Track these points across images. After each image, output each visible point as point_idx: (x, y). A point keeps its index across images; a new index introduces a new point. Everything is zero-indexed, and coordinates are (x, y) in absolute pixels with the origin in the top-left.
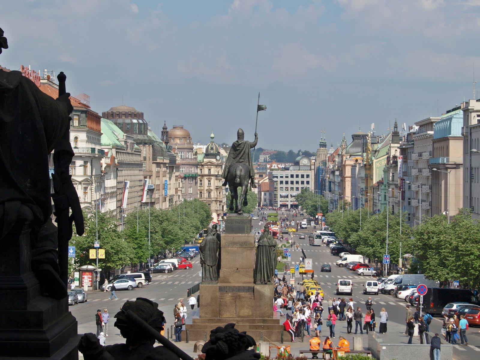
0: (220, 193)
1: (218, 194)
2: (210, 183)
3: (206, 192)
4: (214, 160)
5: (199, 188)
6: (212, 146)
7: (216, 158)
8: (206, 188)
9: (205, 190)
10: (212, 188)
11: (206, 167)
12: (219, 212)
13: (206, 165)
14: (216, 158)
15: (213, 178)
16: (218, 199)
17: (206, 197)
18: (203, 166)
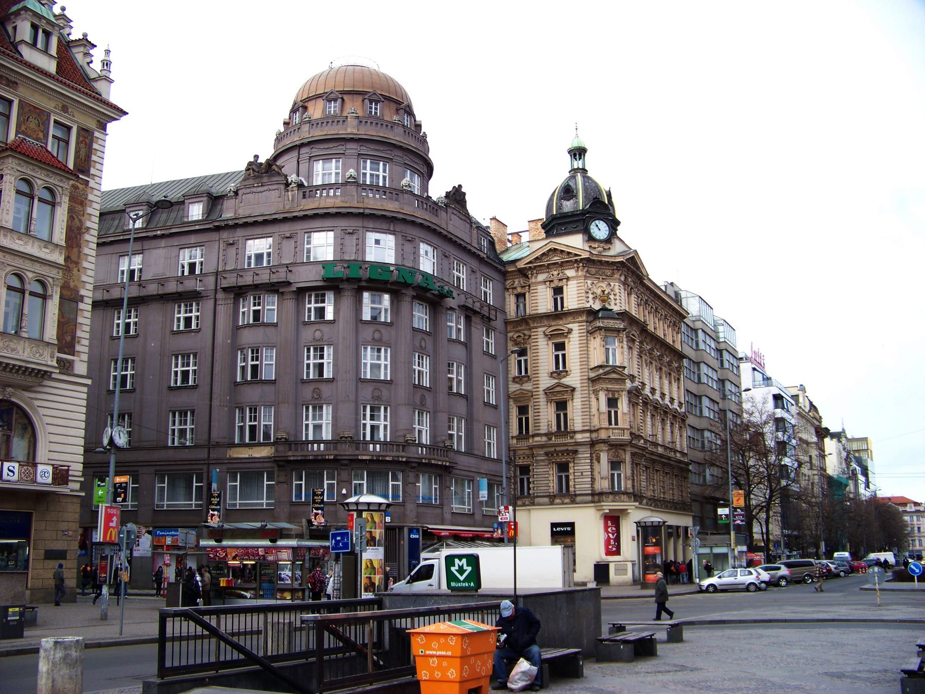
0: (612, 402)
1: (604, 407)
2: (564, 356)
3: (542, 399)
4: (575, 242)
5: (513, 387)
6: (571, 184)
7: (586, 232)
8: (545, 382)
9: (541, 393)
10: (574, 379)
11: (541, 277)
12: (609, 505)
13: (540, 269)
14: (586, 232)
15: (576, 329)
16: (603, 435)
17: (543, 430)
18: (523, 273)
